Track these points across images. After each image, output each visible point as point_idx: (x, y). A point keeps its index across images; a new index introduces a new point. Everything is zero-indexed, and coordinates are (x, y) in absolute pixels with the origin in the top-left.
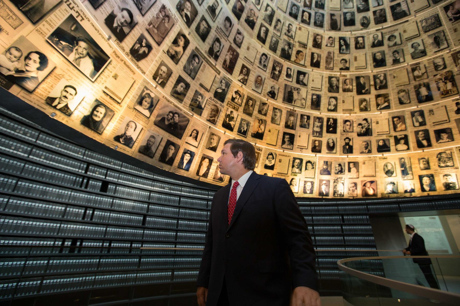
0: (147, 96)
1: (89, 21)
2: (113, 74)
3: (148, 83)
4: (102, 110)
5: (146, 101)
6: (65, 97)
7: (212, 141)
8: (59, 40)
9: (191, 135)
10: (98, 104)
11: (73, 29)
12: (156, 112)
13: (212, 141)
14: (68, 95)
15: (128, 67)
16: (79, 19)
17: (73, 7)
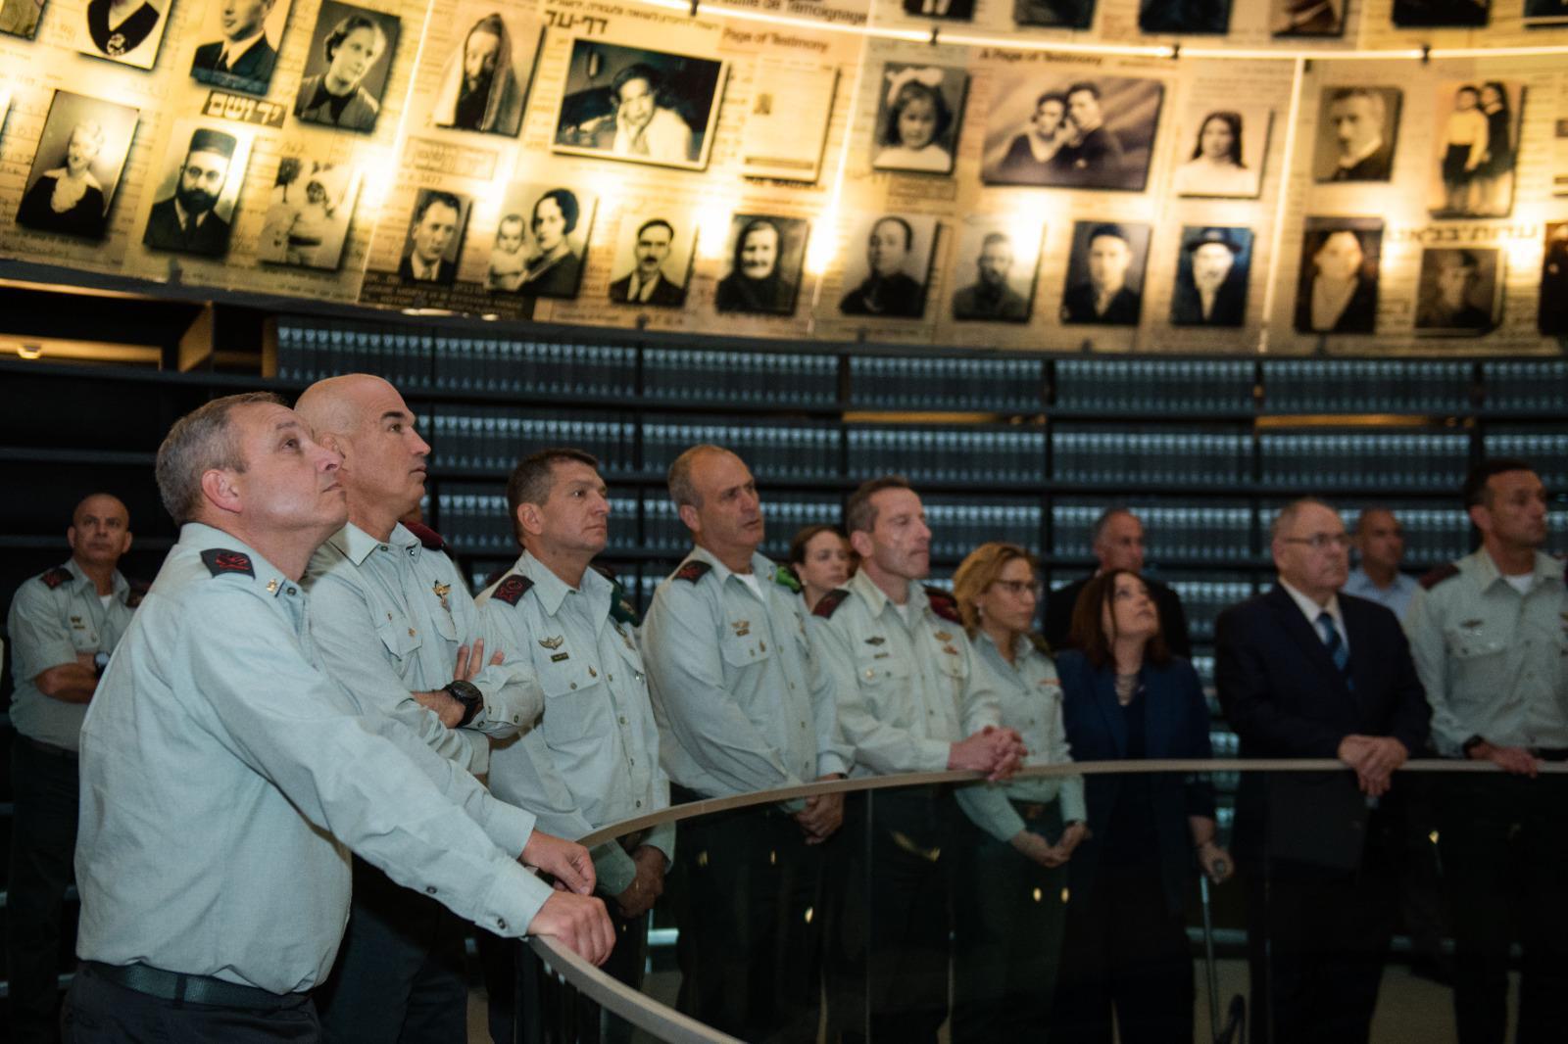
0: (907, 95)
1: (620, 11)
2: (753, 103)
3: (894, 44)
4: (765, 238)
5: (912, 118)
6: (650, 260)
7: (1347, 129)
8: (578, 126)
9: (1198, 153)
10: (748, 224)
11: (593, 70)
12: (973, 135)
13: (1347, 129)
14: (653, 251)
15: (792, 42)
16: (596, 36)
17: (572, 17)
